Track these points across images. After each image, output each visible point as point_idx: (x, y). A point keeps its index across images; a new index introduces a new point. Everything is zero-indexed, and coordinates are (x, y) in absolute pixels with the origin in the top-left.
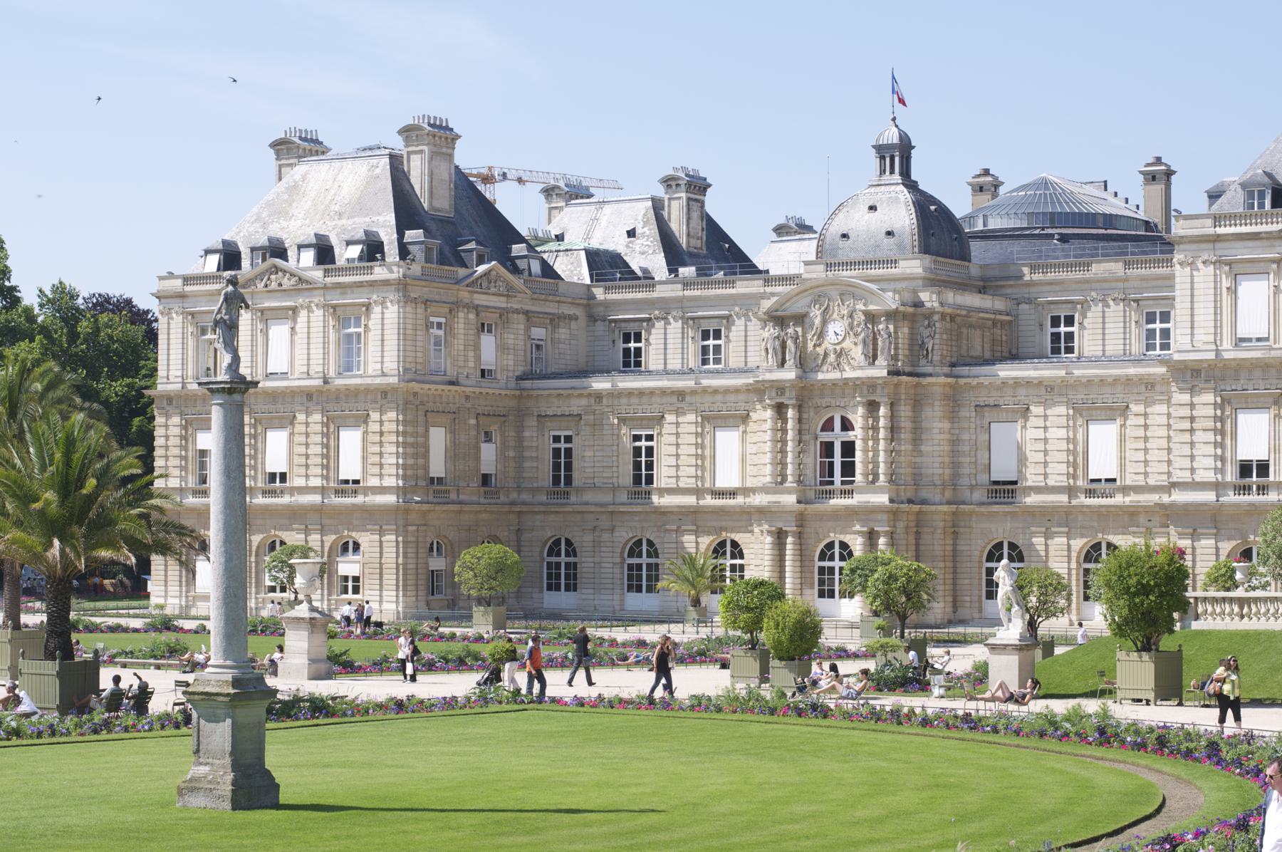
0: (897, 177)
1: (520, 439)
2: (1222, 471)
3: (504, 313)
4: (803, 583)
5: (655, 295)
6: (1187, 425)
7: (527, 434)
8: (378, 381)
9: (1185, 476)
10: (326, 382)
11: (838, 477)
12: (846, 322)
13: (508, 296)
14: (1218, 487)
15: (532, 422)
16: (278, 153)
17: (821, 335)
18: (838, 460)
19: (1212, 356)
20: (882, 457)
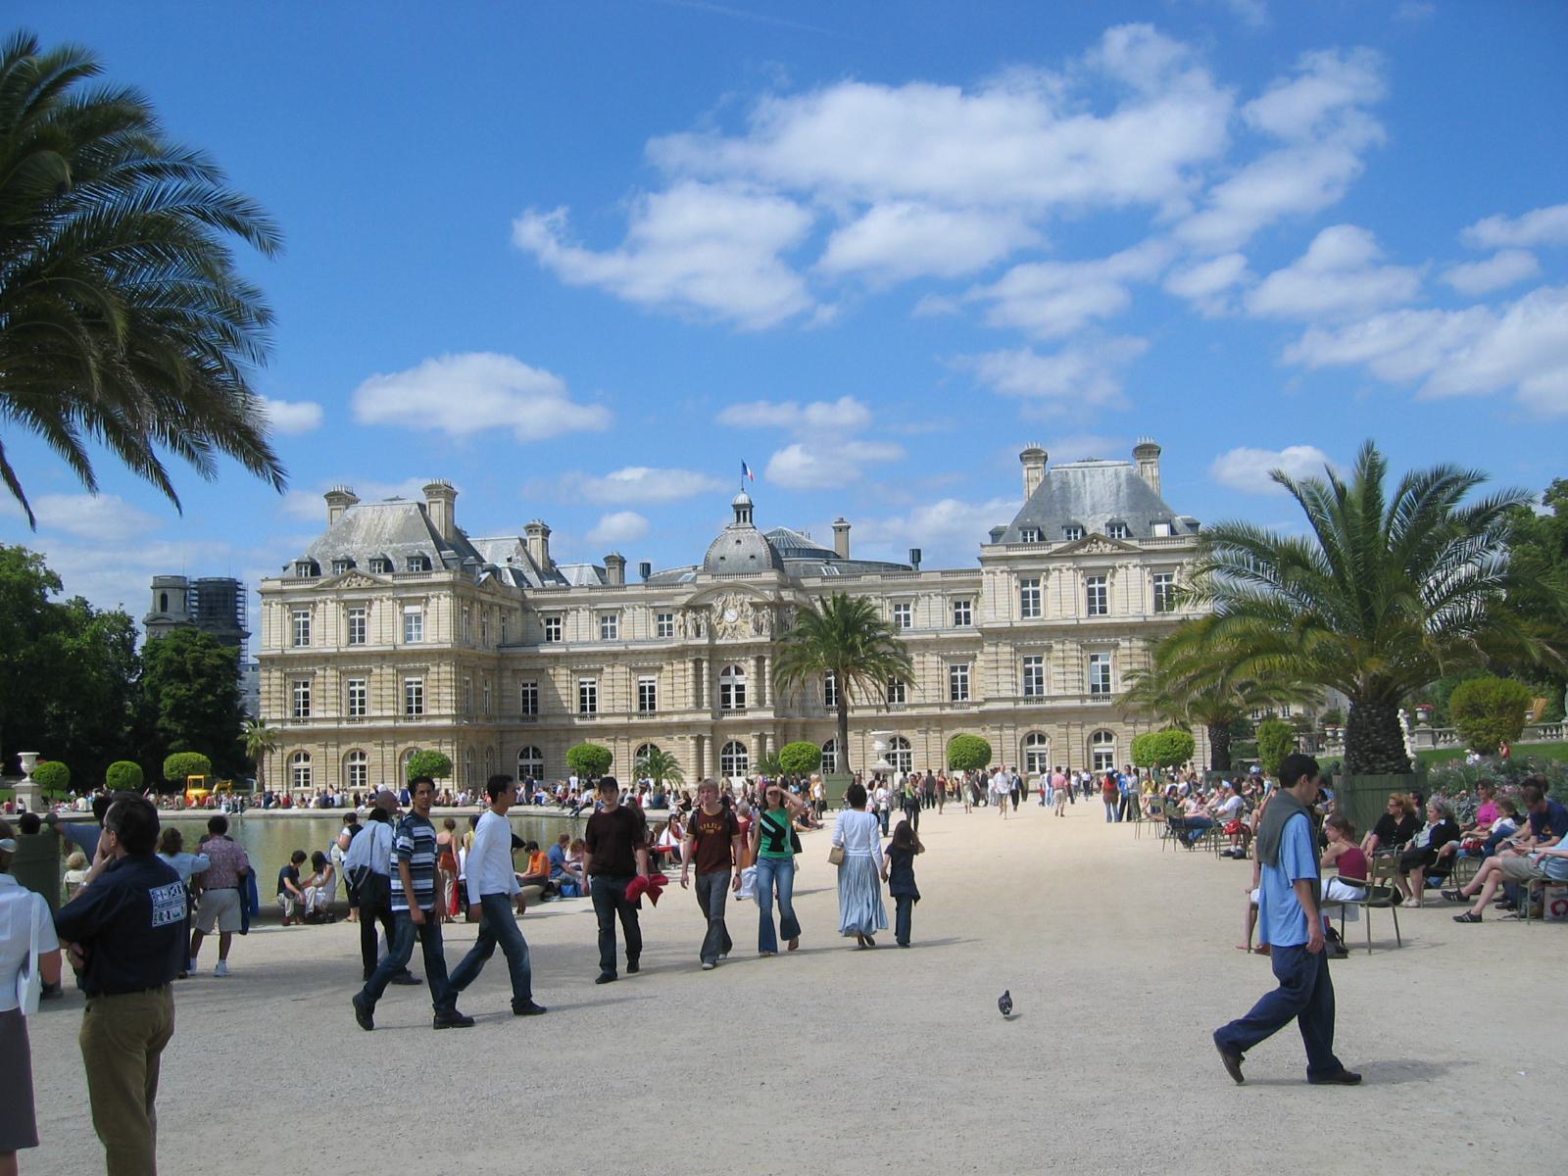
0: (748, 524)
1: (500, 685)
2: (1017, 691)
3: (491, 605)
4: (715, 768)
5: (570, 595)
6: (995, 665)
7: (505, 681)
8: (435, 647)
9: (995, 694)
10: (395, 647)
11: (733, 704)
12: (739, 608)
13: (493, 595)
14: (1015, 700)
15: (508, 674)
16: (330, 502)
17: (722, 616)
18: (733, 692)
19: (1008, 625)
20: (768, 690)
